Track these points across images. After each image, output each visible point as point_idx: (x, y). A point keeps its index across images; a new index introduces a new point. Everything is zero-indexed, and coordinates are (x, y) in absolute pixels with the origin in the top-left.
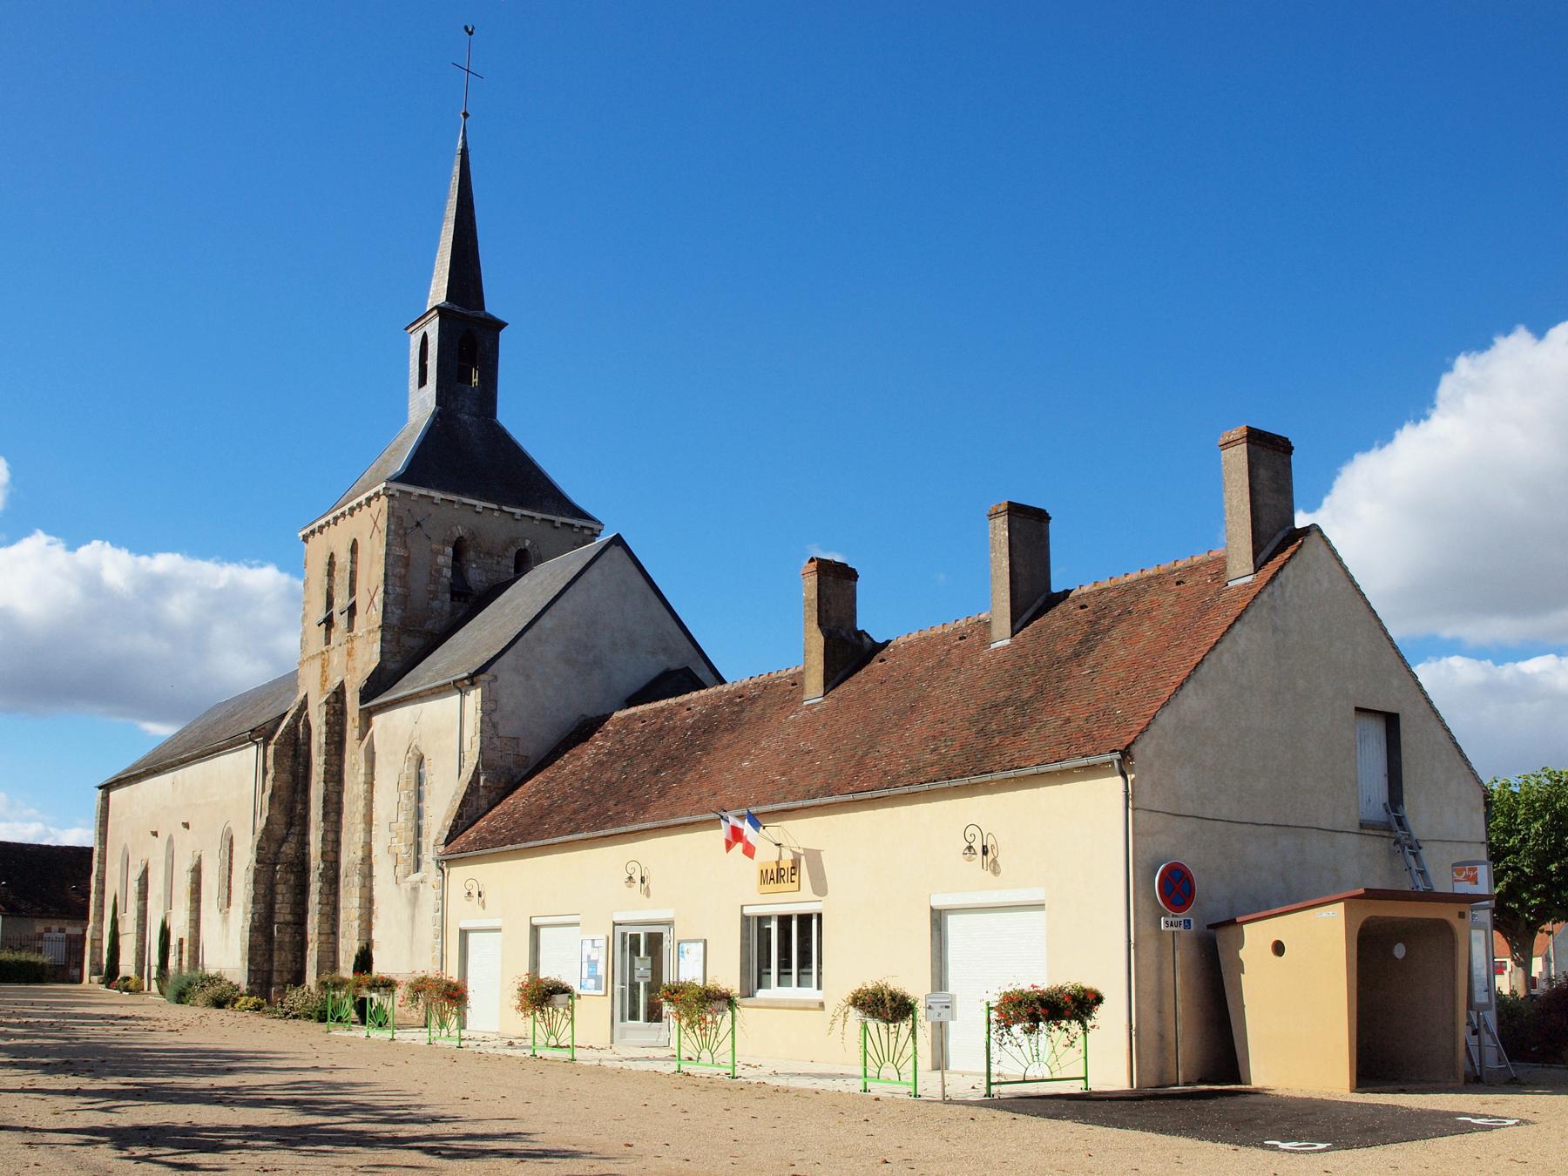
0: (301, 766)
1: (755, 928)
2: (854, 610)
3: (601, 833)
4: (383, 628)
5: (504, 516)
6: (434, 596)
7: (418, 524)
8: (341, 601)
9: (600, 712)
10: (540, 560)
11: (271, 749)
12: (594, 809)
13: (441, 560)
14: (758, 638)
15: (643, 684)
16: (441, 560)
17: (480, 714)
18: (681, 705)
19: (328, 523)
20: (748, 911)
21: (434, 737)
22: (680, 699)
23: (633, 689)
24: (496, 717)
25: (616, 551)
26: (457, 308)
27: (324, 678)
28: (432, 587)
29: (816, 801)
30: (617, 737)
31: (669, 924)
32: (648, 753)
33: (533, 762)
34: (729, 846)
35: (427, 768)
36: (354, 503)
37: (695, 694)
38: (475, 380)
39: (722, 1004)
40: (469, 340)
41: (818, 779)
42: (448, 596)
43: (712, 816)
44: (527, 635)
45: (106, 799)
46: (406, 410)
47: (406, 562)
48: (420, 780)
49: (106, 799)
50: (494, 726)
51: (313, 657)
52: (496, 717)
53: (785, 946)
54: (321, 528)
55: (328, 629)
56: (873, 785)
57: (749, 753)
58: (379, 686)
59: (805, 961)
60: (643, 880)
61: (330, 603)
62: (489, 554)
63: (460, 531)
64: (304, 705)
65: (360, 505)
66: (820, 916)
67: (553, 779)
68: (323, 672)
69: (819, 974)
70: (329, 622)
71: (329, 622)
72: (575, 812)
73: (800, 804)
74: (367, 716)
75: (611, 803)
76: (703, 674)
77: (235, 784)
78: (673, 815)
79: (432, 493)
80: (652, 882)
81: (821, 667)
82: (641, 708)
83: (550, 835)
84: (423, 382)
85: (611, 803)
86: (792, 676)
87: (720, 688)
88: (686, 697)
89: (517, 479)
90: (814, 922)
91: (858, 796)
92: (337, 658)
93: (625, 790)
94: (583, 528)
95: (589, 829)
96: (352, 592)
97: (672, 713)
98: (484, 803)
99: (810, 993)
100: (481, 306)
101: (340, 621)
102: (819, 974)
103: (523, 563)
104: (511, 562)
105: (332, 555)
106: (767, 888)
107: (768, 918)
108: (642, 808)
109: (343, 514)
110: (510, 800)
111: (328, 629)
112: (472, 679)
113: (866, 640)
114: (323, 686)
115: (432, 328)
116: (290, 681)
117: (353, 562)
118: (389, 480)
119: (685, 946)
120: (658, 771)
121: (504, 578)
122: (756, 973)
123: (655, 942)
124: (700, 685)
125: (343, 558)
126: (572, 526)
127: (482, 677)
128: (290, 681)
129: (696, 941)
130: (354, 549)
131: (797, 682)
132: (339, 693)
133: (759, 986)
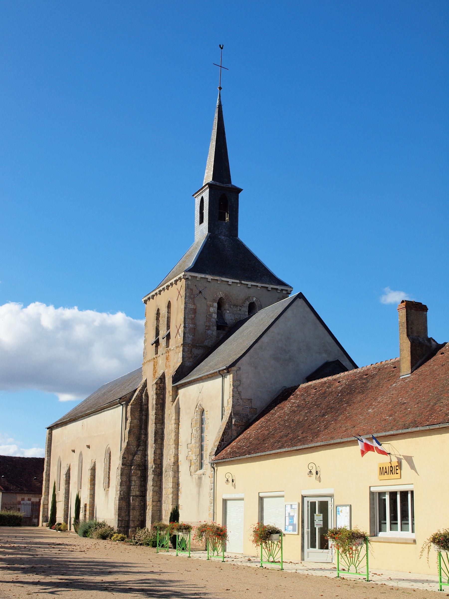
0: (144, 415)
1: (377, 499)
2: (426, 328)
3: (295, 448)
4: (184, 345)
5: (243, 286)
6: (208, 328)
7: (200, 292)
8: (163, 332)
9: (293, 385)
10: (261, 308)
11: (129, 407)
12: (291, 436)
13: (212, 310)
14: (374, 343)
15: (314, 369)
16: (212, 310)
17: (232, 388)
18: (335, 380)
19: (156, 294)
20: (373, 489)
21: (209, 400)
22: (335, 377)
23: (309, 373)
24: (240, 389)
25: (300, 302)
26: (218, 184)
27: (155, 371)
28: (208, 324)
29: (409, 430)
30: (302, 398)
31: (331, 496)
32: (318, 406)
33: (259, 411)
34: (363, 453)
35: (205, 416)
36: (168, 283)
37: (342, 374)
38: (227, 219)
39: (361, 540)
40: (224, 200)
41: (410, 418)
42: (215, 328)
43: (353, 438)
44: (256, 346)
45: (50, 434)
46: (194, 235)
47: (195, 311)
48: (202, 422)
49: (50, 434)
50: (239, 393)
51: (149, 361)
52: (240, 389)
53: (394, 508)
54: (153, 296)
55: (157, 346)
56: (441, 420)
57: (371, 405)
58: (182, 374)
59: (405, 516)
60: (317, 473)
61: (157, 334)
62: (236, 306)
63: (220, 294)
64: (145, 385)
65: (172, 284)
66: (412, 492)
67: (270, 420)
68: (154, 368)
69: (413, 524)
70: (157, 343)
71: (157, 343)
72: (281, 437)
73: (400, 431)
74: (176, 390)
75: (300, 432)
76: (346, 363)
77: (112, 425)
78: (332, 438)
79: (207, 276)
80: (321, 474)
81: (409, 358)
82: (314, 382)
83: (268, 449)
84: (201, 221)
85: (300, 432)
86: (393, 363)
87: (355, 370)
88: (338, 376)
89: (249, 267)
90: (409, 496)
91: (432, 427)
92: (161, 361)
93: (307, 425)
94: (282, 290)
95: (289, 446)
96: (168, 327)
97: (330, 384)
98: (235, 433)
99: (408, 535)
100: (229, 181)
101: (163, 342)
102: (413, 524)
103: (252, 309)
104: (246, 309)
105: (158, 310)
106: (383, 477)
107: (384, 493)
108: (316, 434)
109: (164, 289)
110: (248, 431)
111: (157, 346)
112: (228, 370)
113: (433, 343)
114: (154, 375)
115: (206, 195)
116: (139, 373)
117: (169, 312)
118: (186, 271)
119: (340, 508)
120: (324, 415)
121: (243, 317)
122: (378, 524)
123: (324, 507)
124: (345, 369)
125: (163, 311)
126: (277, 289)
127: (233, 368)
128: (139, 373)
129: (346, 506)
130: (169, 306)
131: (396, 366)
132: (162, 379)
133: (380, 531)
